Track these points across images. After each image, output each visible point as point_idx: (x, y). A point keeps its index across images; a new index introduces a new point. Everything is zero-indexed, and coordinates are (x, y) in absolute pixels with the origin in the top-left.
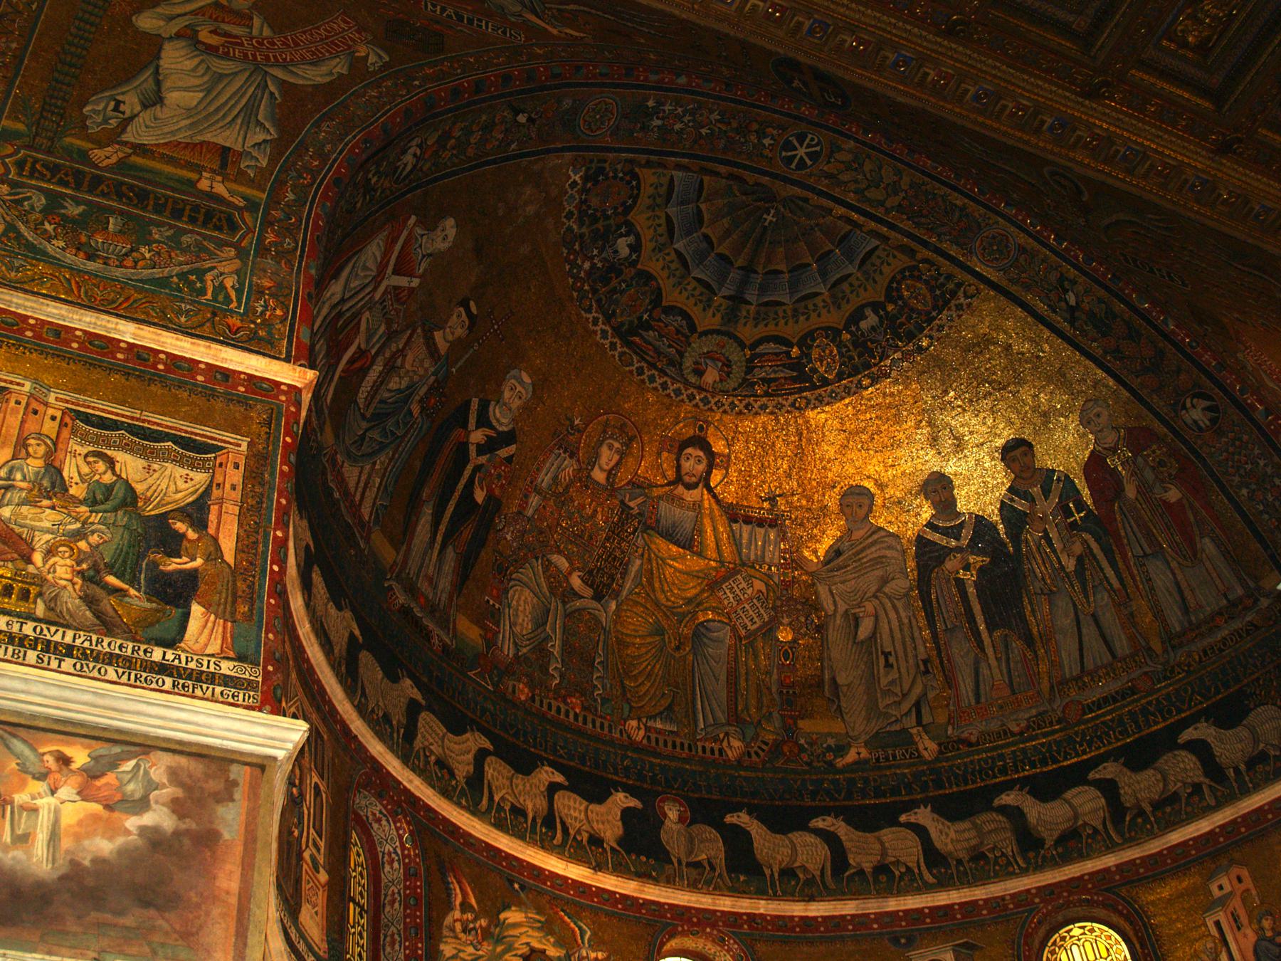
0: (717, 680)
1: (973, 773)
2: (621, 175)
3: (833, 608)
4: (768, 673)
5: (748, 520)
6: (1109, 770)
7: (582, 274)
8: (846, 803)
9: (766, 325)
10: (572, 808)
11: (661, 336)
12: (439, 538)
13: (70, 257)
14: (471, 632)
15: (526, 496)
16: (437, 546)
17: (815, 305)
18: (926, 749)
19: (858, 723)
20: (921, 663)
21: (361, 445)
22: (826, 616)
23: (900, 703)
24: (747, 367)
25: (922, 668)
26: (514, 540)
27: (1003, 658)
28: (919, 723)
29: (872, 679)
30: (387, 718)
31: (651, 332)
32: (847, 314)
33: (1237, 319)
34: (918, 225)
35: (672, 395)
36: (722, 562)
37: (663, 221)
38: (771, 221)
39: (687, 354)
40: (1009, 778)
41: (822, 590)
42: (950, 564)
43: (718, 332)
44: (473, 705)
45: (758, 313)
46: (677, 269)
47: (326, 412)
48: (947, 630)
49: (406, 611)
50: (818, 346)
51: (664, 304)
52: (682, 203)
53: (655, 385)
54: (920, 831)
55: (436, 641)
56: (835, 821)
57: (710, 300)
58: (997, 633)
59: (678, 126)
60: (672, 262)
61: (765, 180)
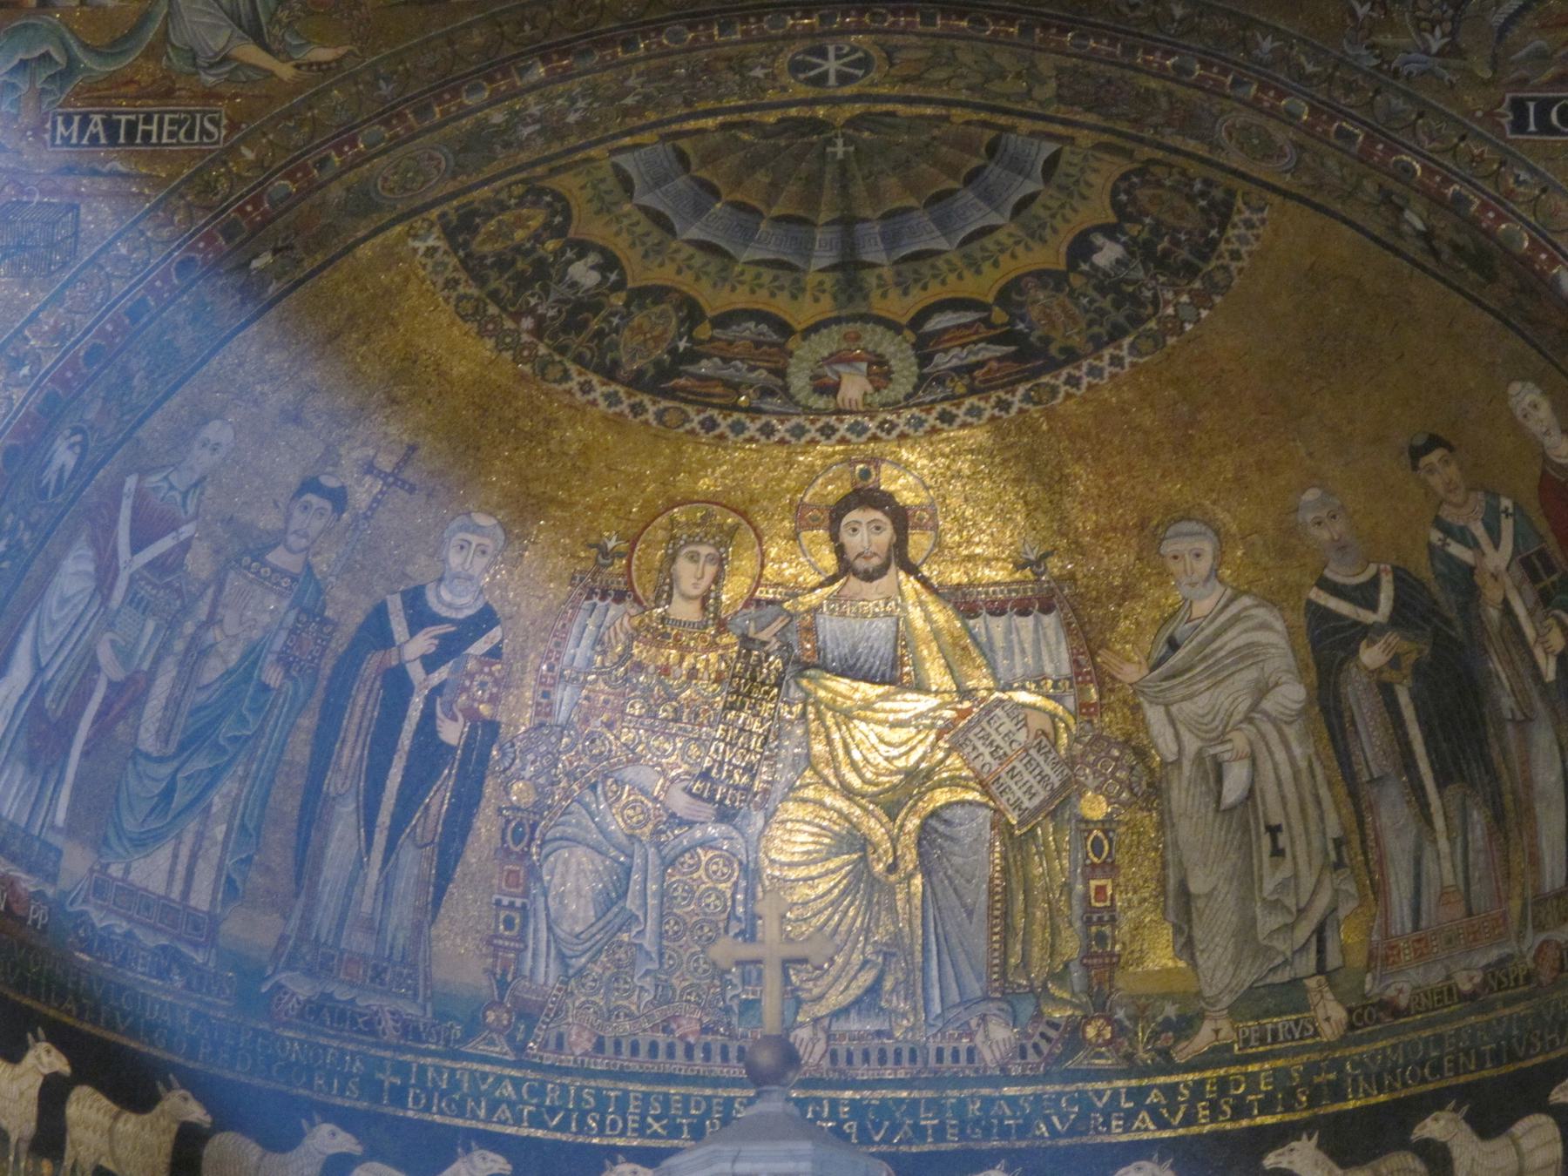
0: (970, 914)
1: (1392, 1072)
2: (513, 201)
3: (1174, 748)
4: (1067, 888)
5: (998, 610)
7: (525, 338)
8: (1181, 1131)
9: (925, 288)
11: (725, 360)
12: (380, 839)
15: (546, 695)
16: (377, 855)
17: (998, 243)
18: (1328, 1019)
20: (1331, 846)
21: (170, 803)
22: (1164, 764)
23: (1291, 927)
24: (917, 356)
25: (1333, 856)
26: (537, 775)
27: (1459, 839)
28: (1321, 969)
29: (1247, 878)
31: (704, 362)
32: (1063, 249)
34: (1108, 117)
35: (788, 437)
36: (965, 694)
37: (638, 216)
38: (846, 153)
39: (792, 370)
40: (1445, 1084)
41: (1155, 715)
42: (1371, 656)
43: (838, 321)
44: (470, 1104)
45: (899, 274)
46: (708, 264)
47: (57, 840)
48: (1372, 781)
49: (316, 1010)
50: (1035, 302)
51: (710, 313)
52: (658, 185)
53: (747, 435)
55: (388, 1023)
56: (1157, 1170)
57: (797, 281)
58: (1453, 790)
59: (572, 118)
60: (691, 257)
61: (793, 112)
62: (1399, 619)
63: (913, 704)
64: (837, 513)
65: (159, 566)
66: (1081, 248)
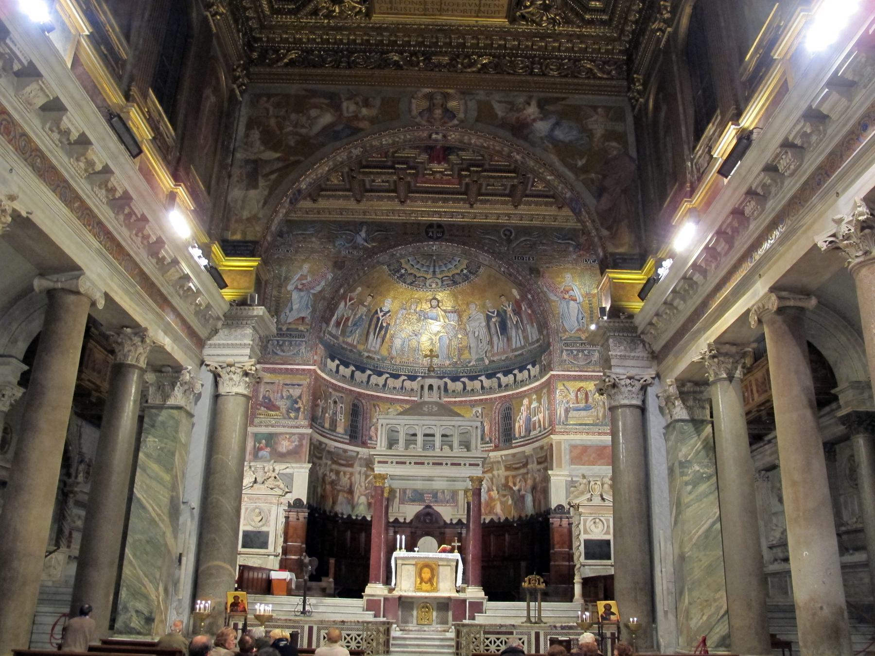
5: (449, 312)
6: (516, 372)
10: (408, 384)
13: (282, 354)
14: (385, 353)
19: (474, 357)
29: (478, 346)
30: (362, 382)
33: (547, 267)
41: (467, 326)
42: (494, 320)
49: (368, 357)
54: (481, 381)
62: (498, 315)
63: (438, 323)
64: (431, 301)
65: (352, 304)
66: (462, 271)
